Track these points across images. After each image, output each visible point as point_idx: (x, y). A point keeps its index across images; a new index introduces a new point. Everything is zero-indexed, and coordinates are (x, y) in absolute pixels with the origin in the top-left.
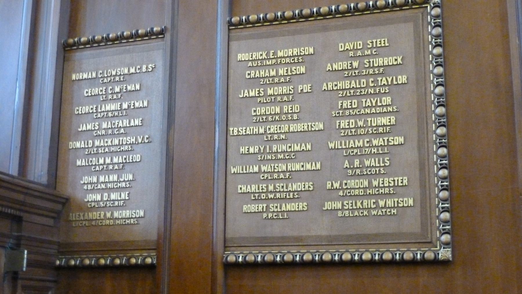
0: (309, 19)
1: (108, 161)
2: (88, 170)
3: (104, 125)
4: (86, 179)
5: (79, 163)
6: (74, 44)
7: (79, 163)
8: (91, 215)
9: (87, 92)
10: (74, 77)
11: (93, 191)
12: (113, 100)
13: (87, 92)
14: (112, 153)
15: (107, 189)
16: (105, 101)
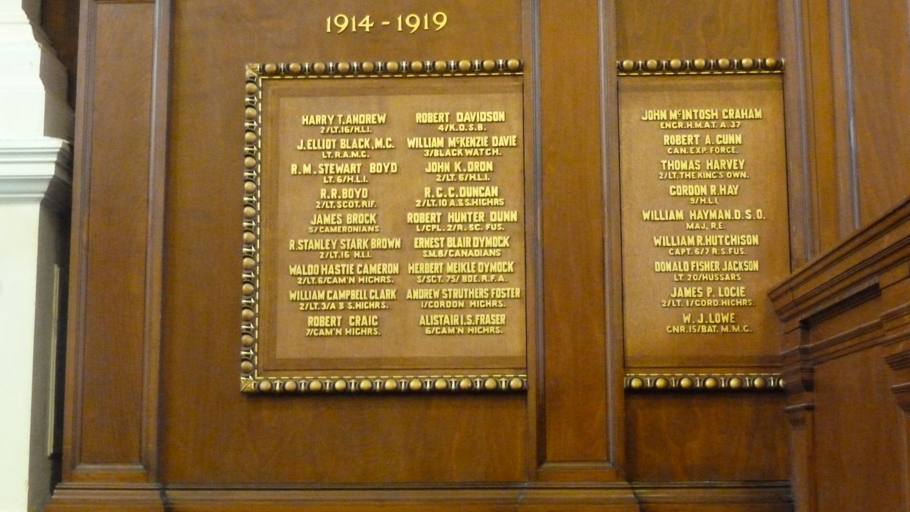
0: (420, 75)
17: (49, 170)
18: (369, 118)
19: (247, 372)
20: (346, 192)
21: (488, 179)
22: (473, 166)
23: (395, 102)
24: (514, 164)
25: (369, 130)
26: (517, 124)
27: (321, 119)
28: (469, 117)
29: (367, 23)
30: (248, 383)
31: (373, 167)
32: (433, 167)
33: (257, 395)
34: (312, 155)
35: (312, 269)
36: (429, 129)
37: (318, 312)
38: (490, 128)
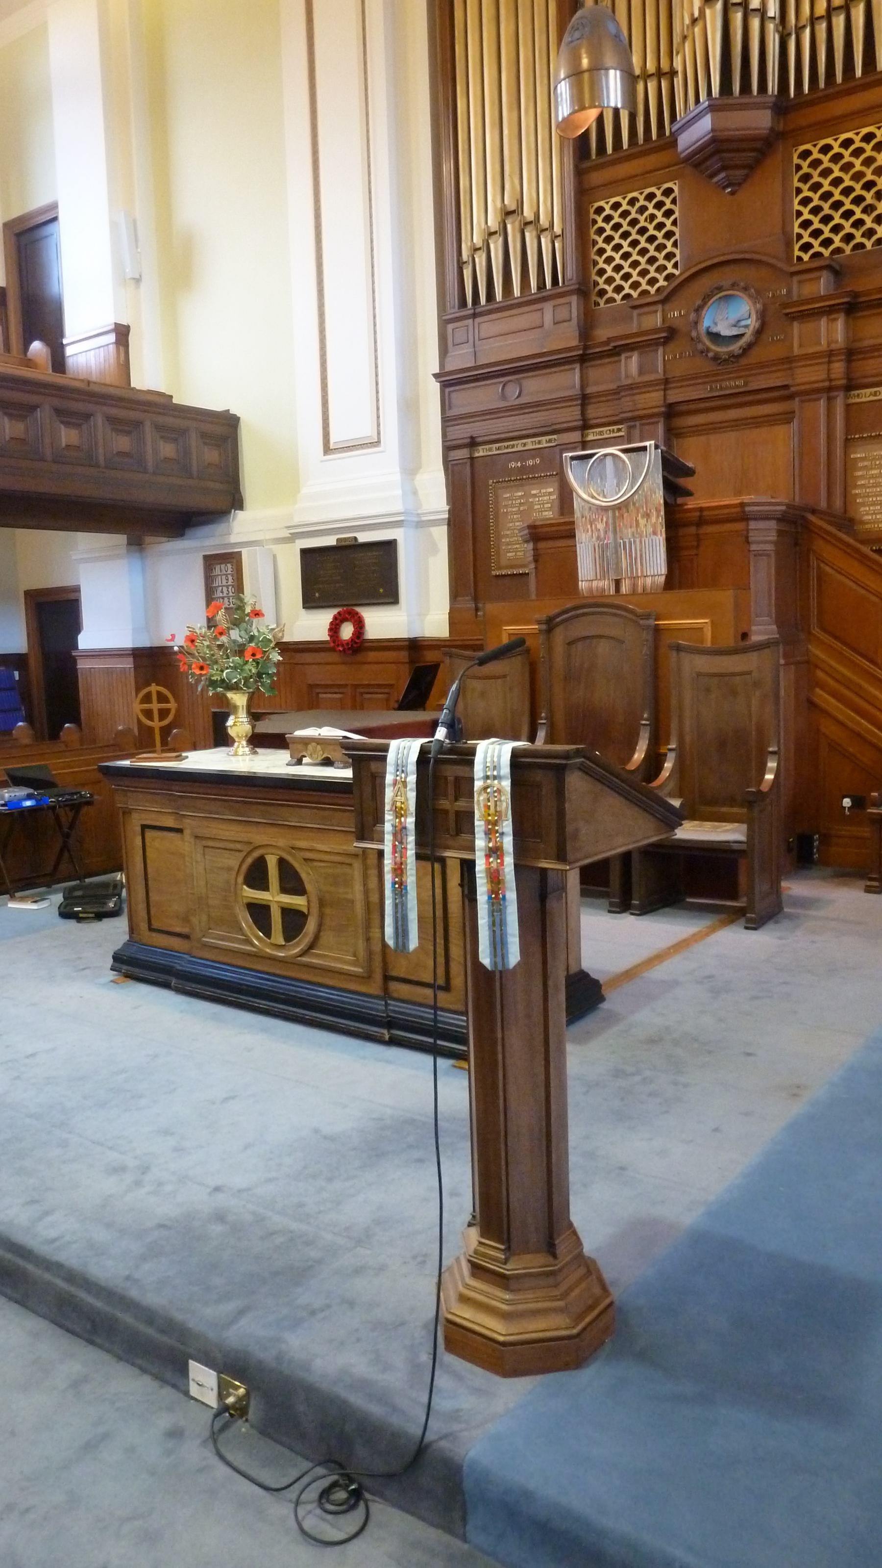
1: (874, 499)
2: (863, 504)
3: (871, 481)
4: (862, 509)
5: (858, 501)
6: (851, 438)
7: (858, 501)
8: (868, 526)
9: (860, 464)
10: (852, 457)
11: (867, 514)
12: (875, 469)
13: (860, 464)
14: (876, 496)
15: (874, 513)
16: (872, 469)
17: (447, 516)
18: (520, 494)
19: (494, 570)
20: (515, 516)
21: (550, 509)
22: (546, 506)
23: (526, 488)
24: (557, 503)
25: (521, 497)
26: (557, 492)
27: (508, 495)
28: (545, 491)
29: (519, 464)
30: (494, 573)
31: (522, 508)
32: (536, 507)
33: (497, 576)
34: (506, 506)
35: (508, 540)
36: (535, 496)
37: (510, 552)
38: (550, 494)
